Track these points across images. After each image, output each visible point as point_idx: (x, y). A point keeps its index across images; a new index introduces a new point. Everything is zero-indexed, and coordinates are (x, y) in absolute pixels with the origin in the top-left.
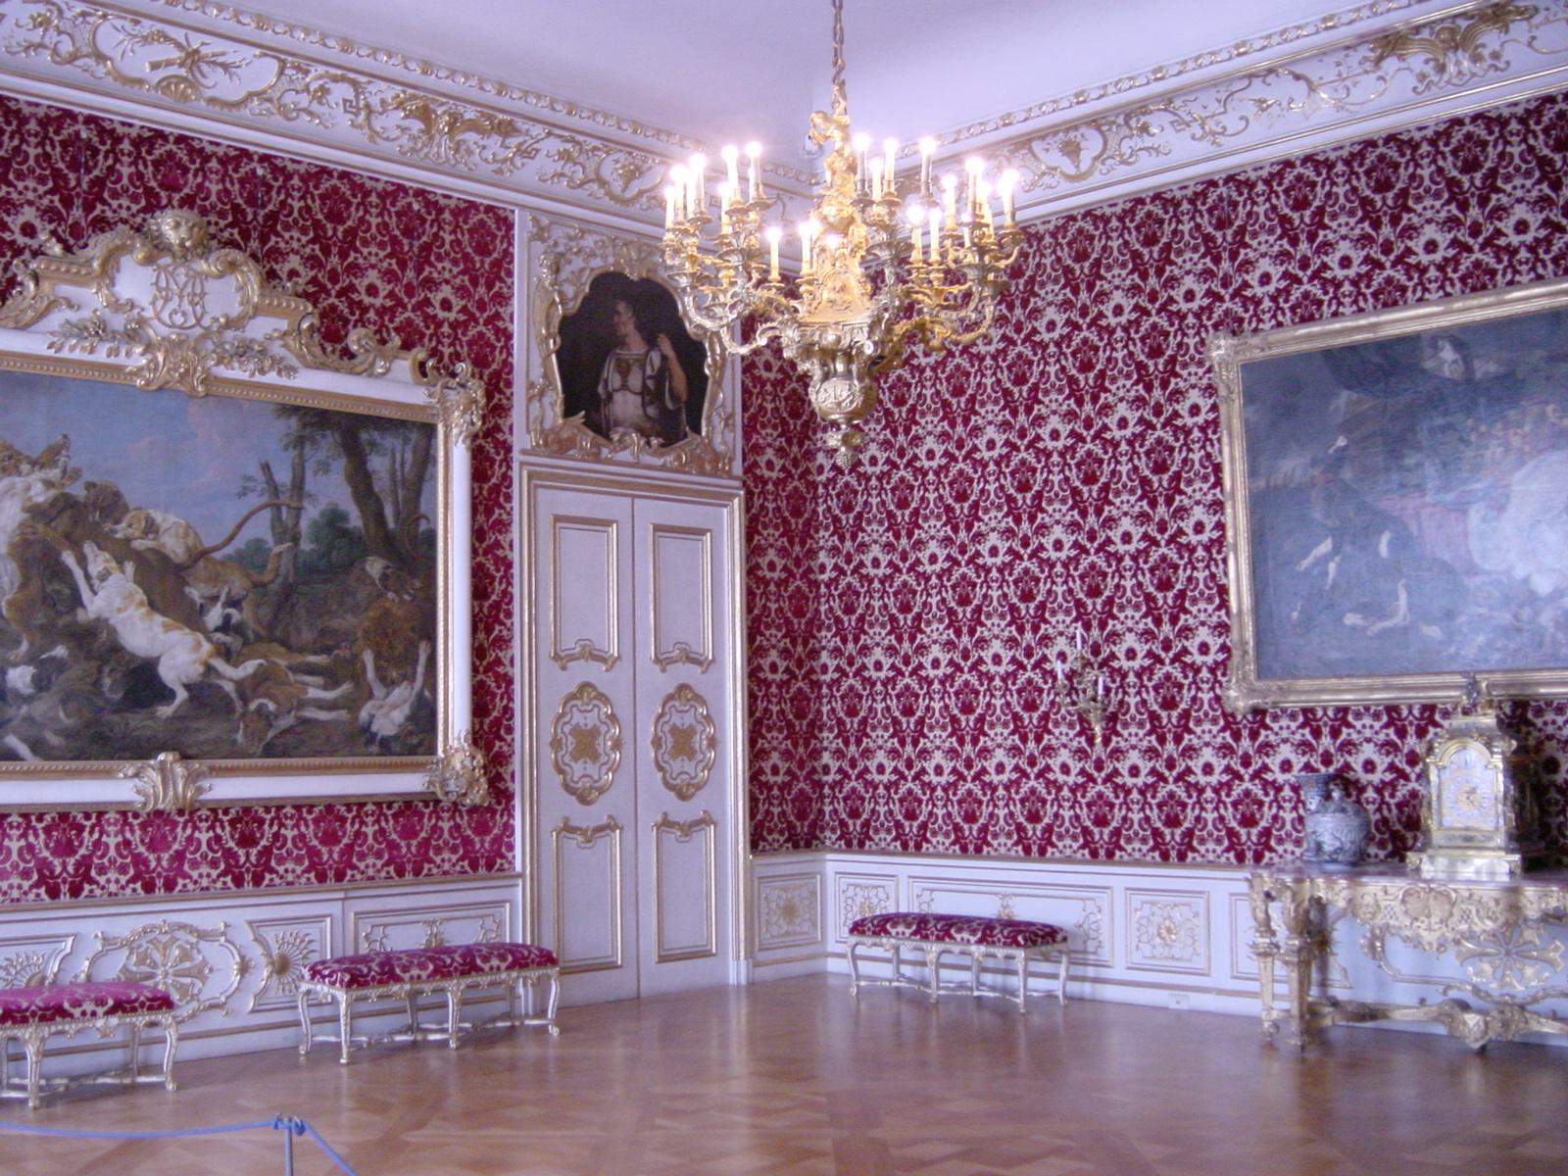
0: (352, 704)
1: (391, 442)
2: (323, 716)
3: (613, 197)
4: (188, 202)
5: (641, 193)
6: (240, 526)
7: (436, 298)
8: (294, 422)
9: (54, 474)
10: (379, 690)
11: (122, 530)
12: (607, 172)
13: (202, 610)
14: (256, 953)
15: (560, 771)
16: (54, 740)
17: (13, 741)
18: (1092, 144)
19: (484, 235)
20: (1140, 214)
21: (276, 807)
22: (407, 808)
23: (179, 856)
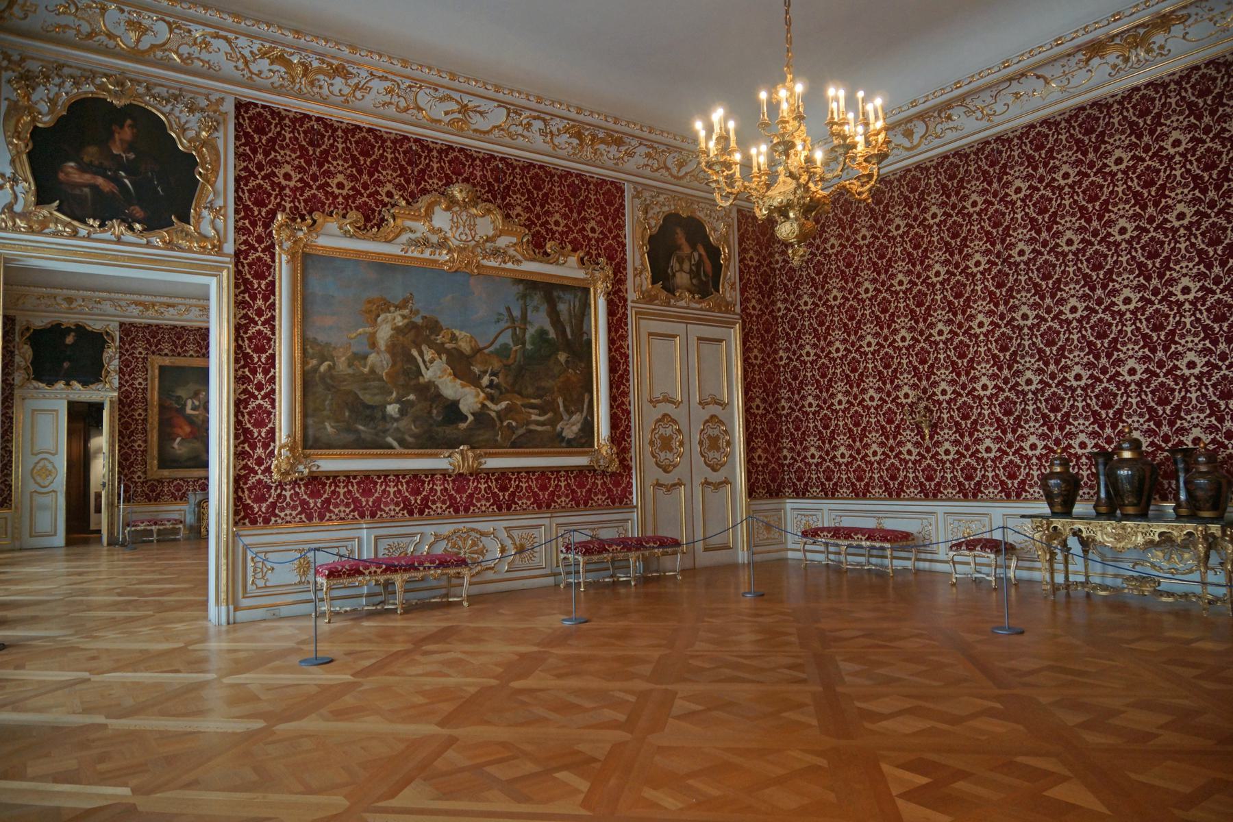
0: (552, 423)
1: (568, 296)
2: (539, 428)
3: (672, 176)
4: (466, 180)
5: (687, 174)
6: (496, 338)
7: (588, 227)
8: (521, 287)
9: (406, 312)
10: (566, 417)
11: (439, 339)
12: (669, 164)
13: (480, 378)
14: (509, 542)
15: (654, 457)
16: (410, 439)
17: (390, 440)
18: (920, 129)
19: (611, 194)
20: (946, 164)
21: (517, 471)
22: (580, 472)
23: (471, 496)
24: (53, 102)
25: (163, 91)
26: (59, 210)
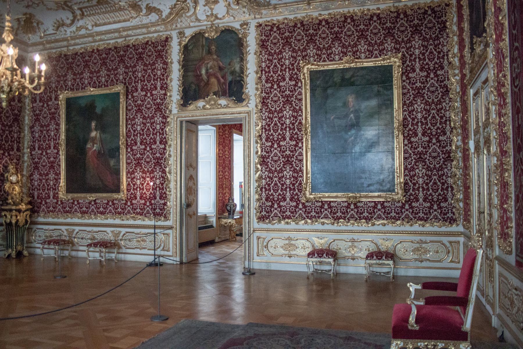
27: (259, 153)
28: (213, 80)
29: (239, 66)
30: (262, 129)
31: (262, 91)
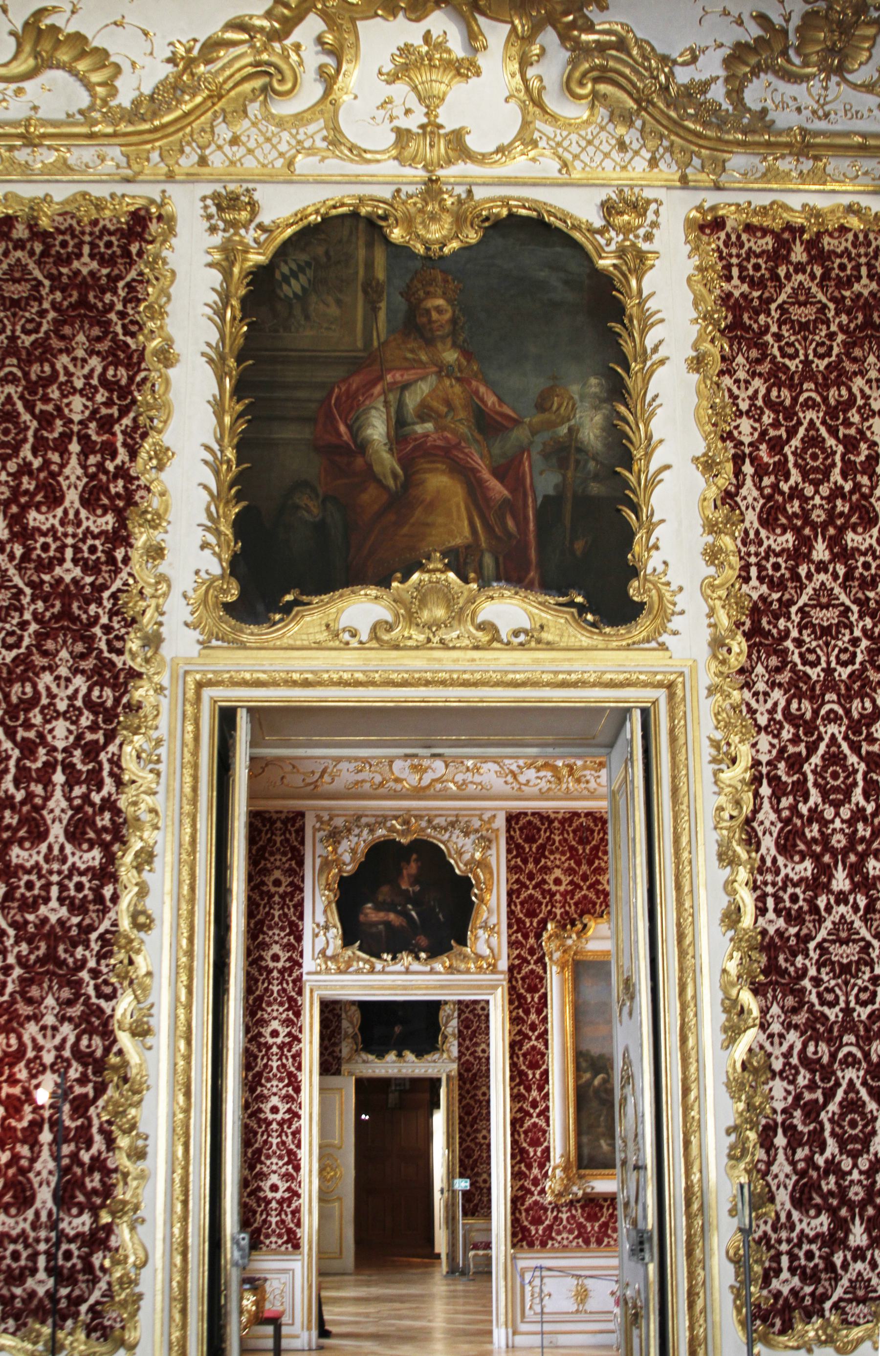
24: (353, 851)
25: (441, 821)
26: (360, 949)
27: (747, 921)
28: (439, 482)
29: (598, 418)
30: (757, 780)
31: (746, 567)
